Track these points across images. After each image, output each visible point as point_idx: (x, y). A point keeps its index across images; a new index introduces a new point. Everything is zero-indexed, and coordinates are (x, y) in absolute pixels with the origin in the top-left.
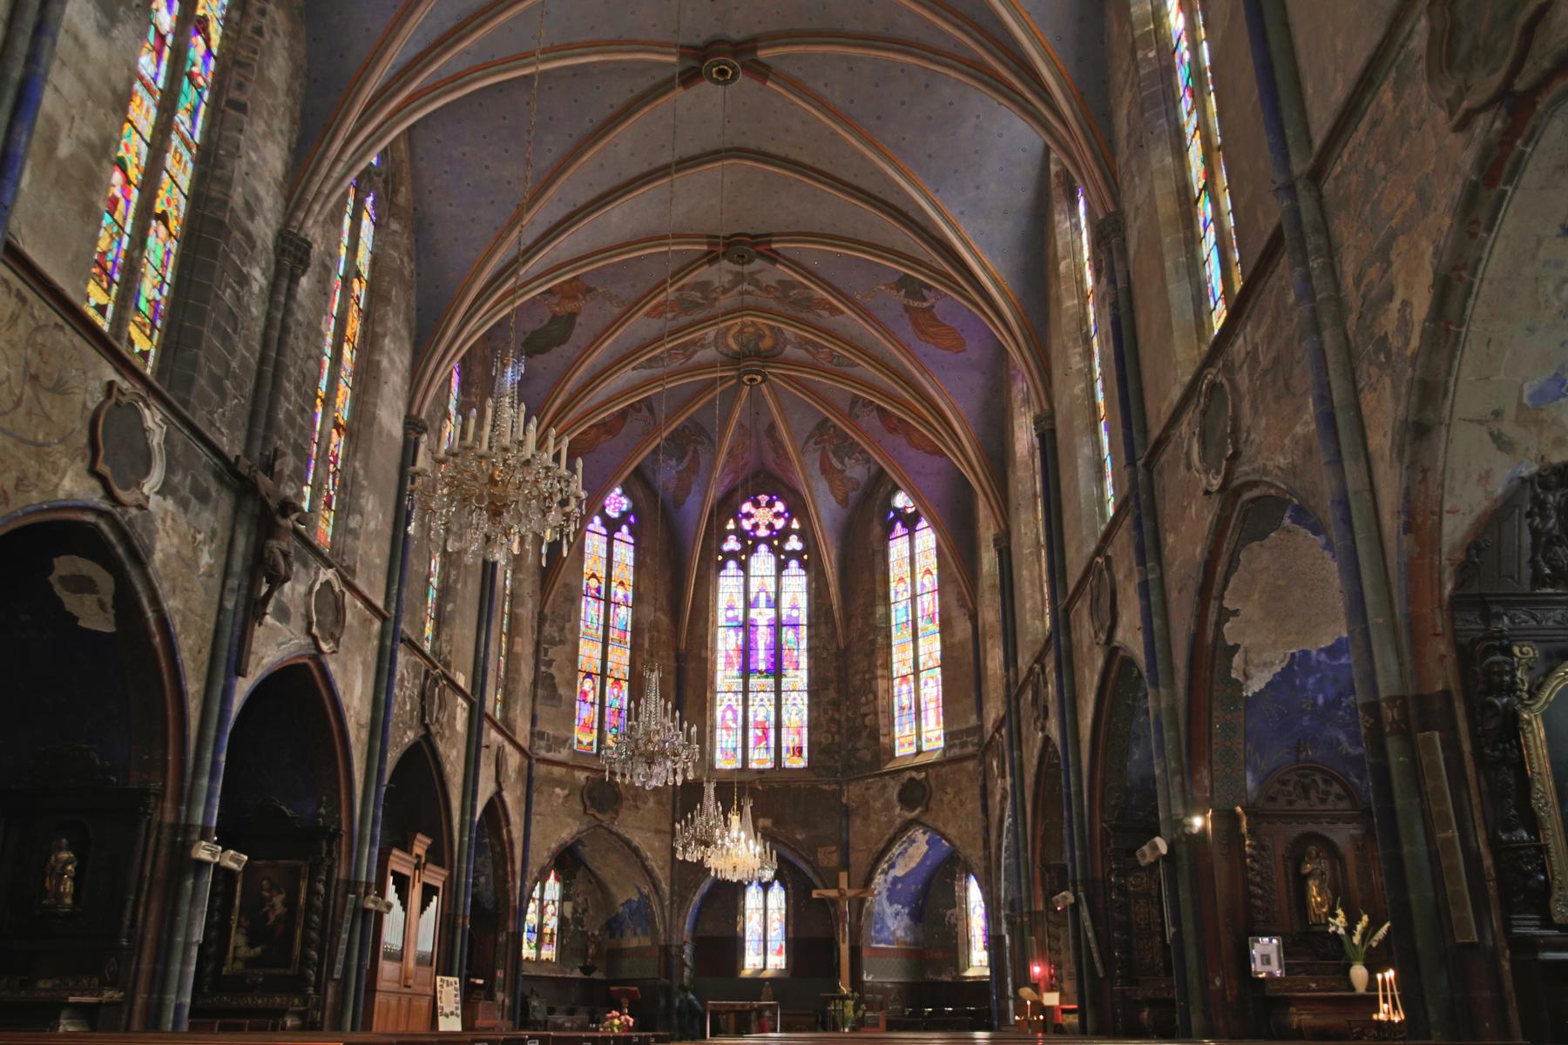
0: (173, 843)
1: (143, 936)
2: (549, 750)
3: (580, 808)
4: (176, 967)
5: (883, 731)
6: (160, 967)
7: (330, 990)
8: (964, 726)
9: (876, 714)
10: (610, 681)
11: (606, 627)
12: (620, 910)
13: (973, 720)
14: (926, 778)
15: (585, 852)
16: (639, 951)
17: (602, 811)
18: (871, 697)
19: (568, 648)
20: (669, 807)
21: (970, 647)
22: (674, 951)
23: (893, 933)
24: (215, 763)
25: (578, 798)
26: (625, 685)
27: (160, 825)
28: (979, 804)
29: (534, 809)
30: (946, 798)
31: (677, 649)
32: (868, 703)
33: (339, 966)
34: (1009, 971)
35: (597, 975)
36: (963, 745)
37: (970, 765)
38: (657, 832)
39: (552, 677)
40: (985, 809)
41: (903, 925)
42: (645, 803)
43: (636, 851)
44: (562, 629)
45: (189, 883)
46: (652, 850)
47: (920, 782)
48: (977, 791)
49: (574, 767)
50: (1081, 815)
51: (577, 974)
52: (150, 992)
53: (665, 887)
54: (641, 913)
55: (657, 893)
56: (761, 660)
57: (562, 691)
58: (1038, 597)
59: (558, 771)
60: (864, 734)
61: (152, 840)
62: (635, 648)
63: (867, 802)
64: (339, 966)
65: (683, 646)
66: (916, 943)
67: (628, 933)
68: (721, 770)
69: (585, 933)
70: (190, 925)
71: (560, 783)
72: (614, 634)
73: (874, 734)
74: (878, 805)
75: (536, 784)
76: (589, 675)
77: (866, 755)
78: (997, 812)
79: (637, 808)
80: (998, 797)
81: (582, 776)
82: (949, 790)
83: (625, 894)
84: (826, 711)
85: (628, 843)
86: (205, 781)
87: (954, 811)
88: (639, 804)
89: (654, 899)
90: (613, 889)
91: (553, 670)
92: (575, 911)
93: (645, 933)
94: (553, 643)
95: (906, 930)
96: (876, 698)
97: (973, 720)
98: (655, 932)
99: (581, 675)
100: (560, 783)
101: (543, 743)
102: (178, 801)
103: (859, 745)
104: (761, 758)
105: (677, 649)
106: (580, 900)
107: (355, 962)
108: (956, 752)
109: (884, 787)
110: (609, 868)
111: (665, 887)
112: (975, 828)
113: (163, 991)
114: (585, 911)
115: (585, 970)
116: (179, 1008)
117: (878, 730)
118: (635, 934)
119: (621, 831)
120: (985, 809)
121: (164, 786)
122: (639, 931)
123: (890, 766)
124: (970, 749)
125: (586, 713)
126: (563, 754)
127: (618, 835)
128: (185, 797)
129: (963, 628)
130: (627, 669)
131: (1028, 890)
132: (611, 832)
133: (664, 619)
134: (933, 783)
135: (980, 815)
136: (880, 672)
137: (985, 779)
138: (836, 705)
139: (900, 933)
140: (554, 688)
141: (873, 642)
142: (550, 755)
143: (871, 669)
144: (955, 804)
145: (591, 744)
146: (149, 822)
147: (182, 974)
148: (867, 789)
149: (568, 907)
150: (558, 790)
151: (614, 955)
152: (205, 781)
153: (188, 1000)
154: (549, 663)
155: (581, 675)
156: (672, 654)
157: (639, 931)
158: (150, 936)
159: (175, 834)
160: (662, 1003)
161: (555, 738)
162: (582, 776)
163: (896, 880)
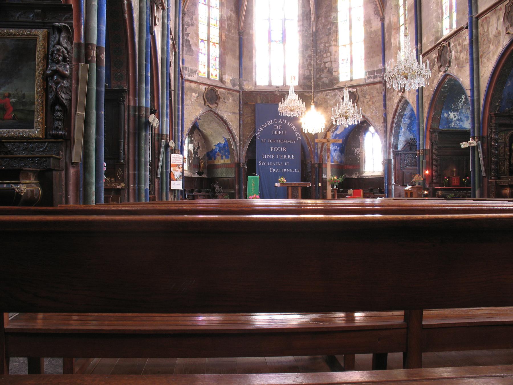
0: (135, 115)
1: (128, 159)
2: (189, 76)
3: (203, 102)
4: (143, 172)
5: (335, 70)
6: (137, 173)
7: (156, 182)
8: (375, 69)
9: (331, 62)
10: (211, 44)
11: (209, 19)
12: (214, 148)
13: (380, 66)
14: (356, 92)
15: (199, 122)
16: (225, 166)
17: (212, 103)
18: (329, 54)
19: (194, 28)
20: (238, 102)
21: (380, 33)
22: (242, 165)
23: (333, 158)
24: (147, 76)
25: (202, 98)
26: (218, 46)
27: (129, 106)
28: (382, 103)
29: (185, 102)
30: (366, 101)
31: (239, 30)
32: (327, 57)
33: (159, 172)
34: (393, 174)
35: (204, 176)
36: (375, 77)
37: (378, 86)
38: (233, 113)
39: (189, 41)
40: (385, 106)
41: (337, 154)
42: (228, 100)
43: (225, 122)
44: (192, 19)
45: (144, 134)
46: (232, 122)
47: (353, 92)
48: (381, 98)
49: (200, 83)
50: (479, 109)
51: (196, 175)
52: (134, 184)
53: (237, 138)
54: (226, 149)
55: (234, 140)
56: (277, 35)
57: (193, 48)
58: (440, 11)
59: (193, 85)
60: (325, 71)
61: (126, 114)
62: (221, 28)
63: (326, 101)
64: (159, 172)
65: (241, 28)
66: (341, 162)
67: (218, 157)
68: (259, 86)
69: (198, 158)
70: (146, 153)
71: (194, 91)
72: (212, 22)
73: (330, 72)
74: (332, 102)
75: (185, 91)
76: (202, 41)
77: (327, 81)
78: (395, 107)
79: (225, 102)
80: (396, 100)
81: (203, 88)
82: (367, 97)
83: (218, 139)
84: (307, 60)
85: (222, 118)
86: (144, 86)
87: (369, 106)
88: (226, 101)
89: (232, 142)
90: (211, 138)
91: (189, 38)
92: (194, 148)
93: (227, 157)
94: (188, 25)
95: (338, 156)
96: (331, 54)
97: (380, 66)
98: (233, 157)
99: (200, 41)
100: (194, 91)
101: (186, 72)
102: (134, 96)
103: (322, 76)
104: (277, 82)
105: (239, 30)
106: (196, 143)
107: (165, 170)
108: (371, 80)
109: (335, 95)
110: (209, 129)
111: (237, 138)
112: (380, 113)
113: (139, 183)
114: (198, 148)
115: (200, 174)
116: (146, 190)
117: (332, 69)
118: (222, 158)
119: (219, 113)
120: (385, 106)
121: (129, 88)
122: (224, 156)
123: (336, 86)
124: (378, 79)
125: (202, 59)
126: (194, 78)
127: (218, 115)
128: (137, 93)
129: (376, 24)
130: (218, 39)
131: (423, 140)
132: (215, 113)
133: (234, 15)
134: (359, 94)
135: (382, 108)
136: (333, 43)
137: (385, 92)
138: (310, 56)
139: (336, 158)
140: (190, 46)
141: (330, 29)
142: (190, 78)
143: (329, 42)
144: (370, 103)
145: (205, 73)
146: (124, 105)
147: (145, 176)
148: (327, 95)
149: (191, 146)
150: (194, 94)
151: (211, 168)
152: (144, 86)
153: (148, 187)
154: (188, 35)
155: (200, 41)
156: (237, 32)
157: (224, 156)
158: (131, 158)
159: (135, 111)
160: (237, 187)
161: (192, 70)
162: (203, 88)
163: (337, 135)
